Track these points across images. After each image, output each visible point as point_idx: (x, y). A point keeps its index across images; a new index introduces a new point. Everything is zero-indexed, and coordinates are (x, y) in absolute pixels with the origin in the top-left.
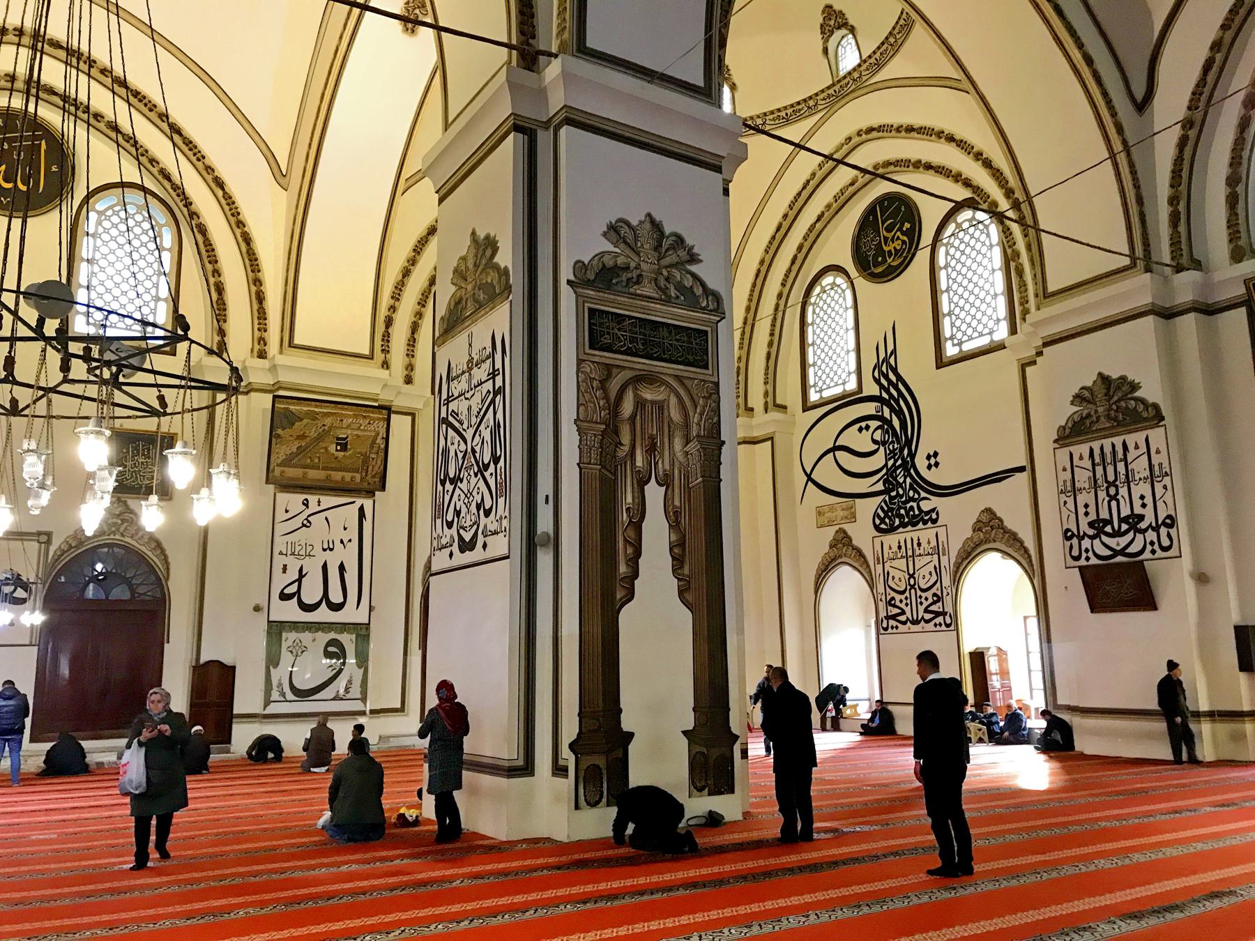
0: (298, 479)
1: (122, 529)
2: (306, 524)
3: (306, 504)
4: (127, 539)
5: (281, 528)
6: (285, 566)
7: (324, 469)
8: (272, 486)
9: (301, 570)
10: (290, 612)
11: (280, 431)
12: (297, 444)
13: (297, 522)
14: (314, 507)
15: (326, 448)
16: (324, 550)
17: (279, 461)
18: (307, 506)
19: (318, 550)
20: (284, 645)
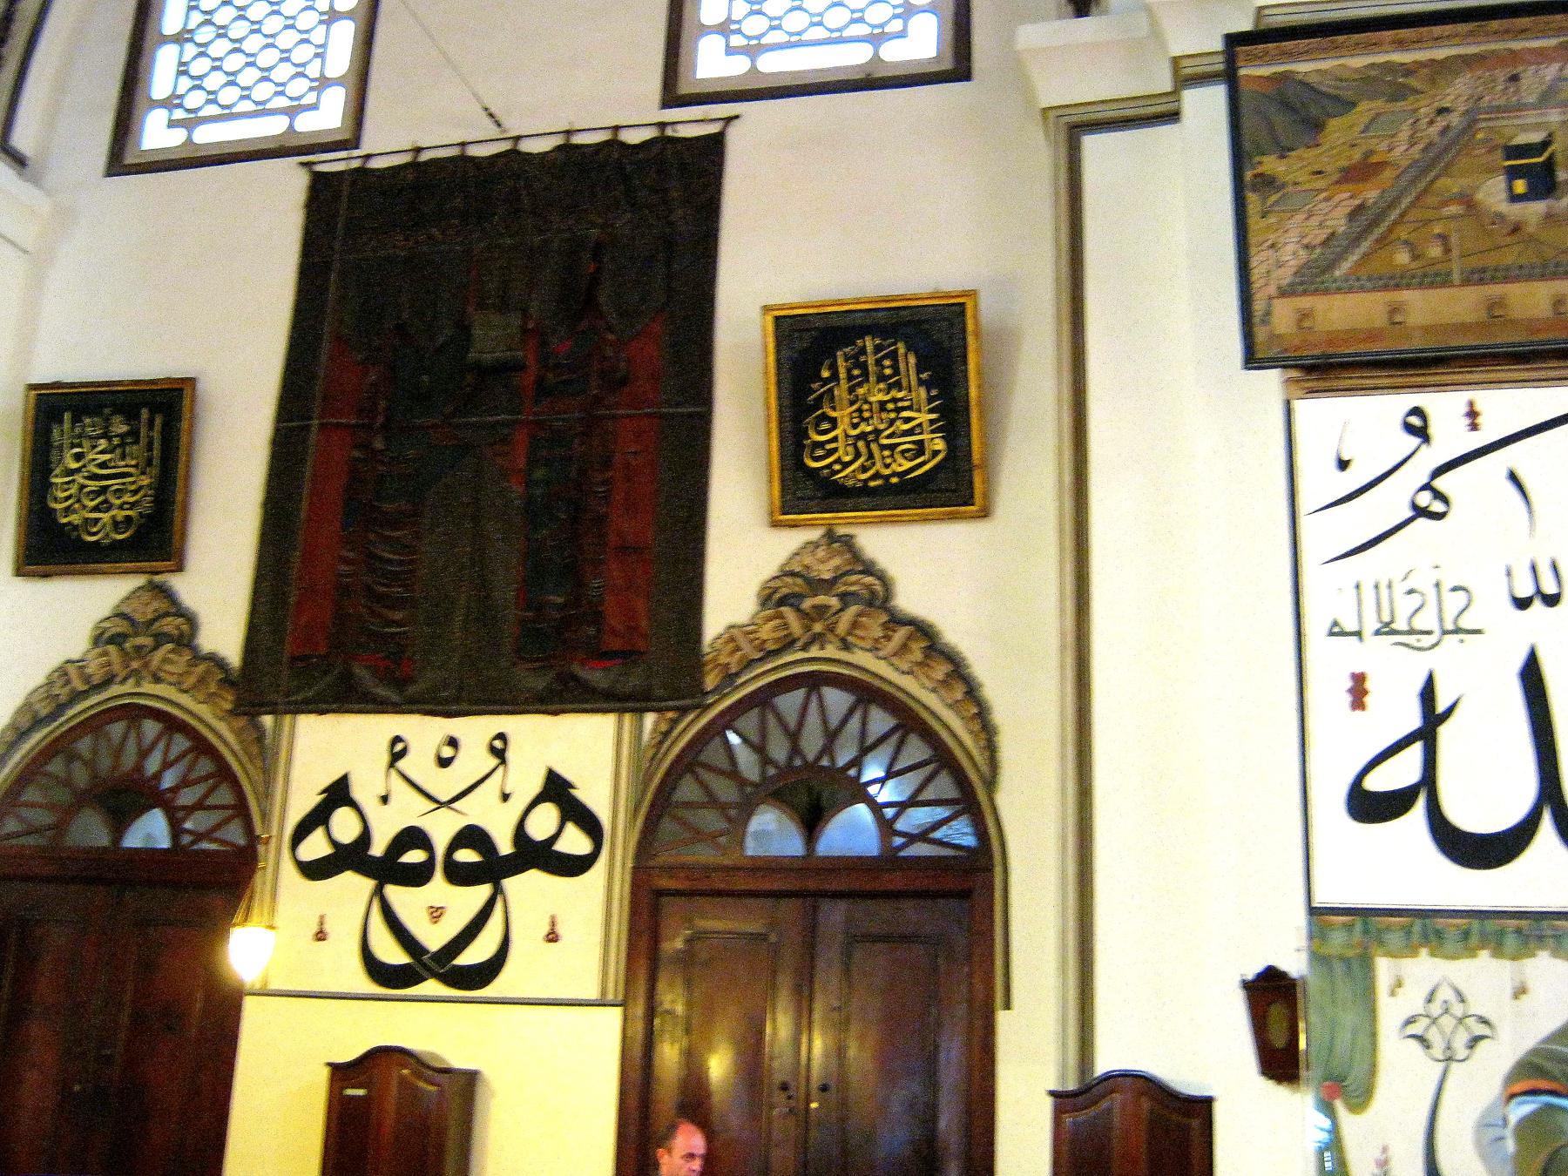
0: (1372, 335)
1: (842, 628)
2: (1429, 508)
3: (1418, 427)
4: (862, 658)
5: (1326, 534)
6: (1359, 681)
7: (1476, 277)
8: (1271, 380)
9: (1428, 694)
10: (1398, 867)
11: (1270, 164)
12: (1345, 201)
13: (1392, 502)
14: (1450, 437)
15: (1468, 201)
16: (1522, 604)
17: (1285, 276)
18: (1422, 433)
19: (1492, 609)
20: (1391, 1012)
